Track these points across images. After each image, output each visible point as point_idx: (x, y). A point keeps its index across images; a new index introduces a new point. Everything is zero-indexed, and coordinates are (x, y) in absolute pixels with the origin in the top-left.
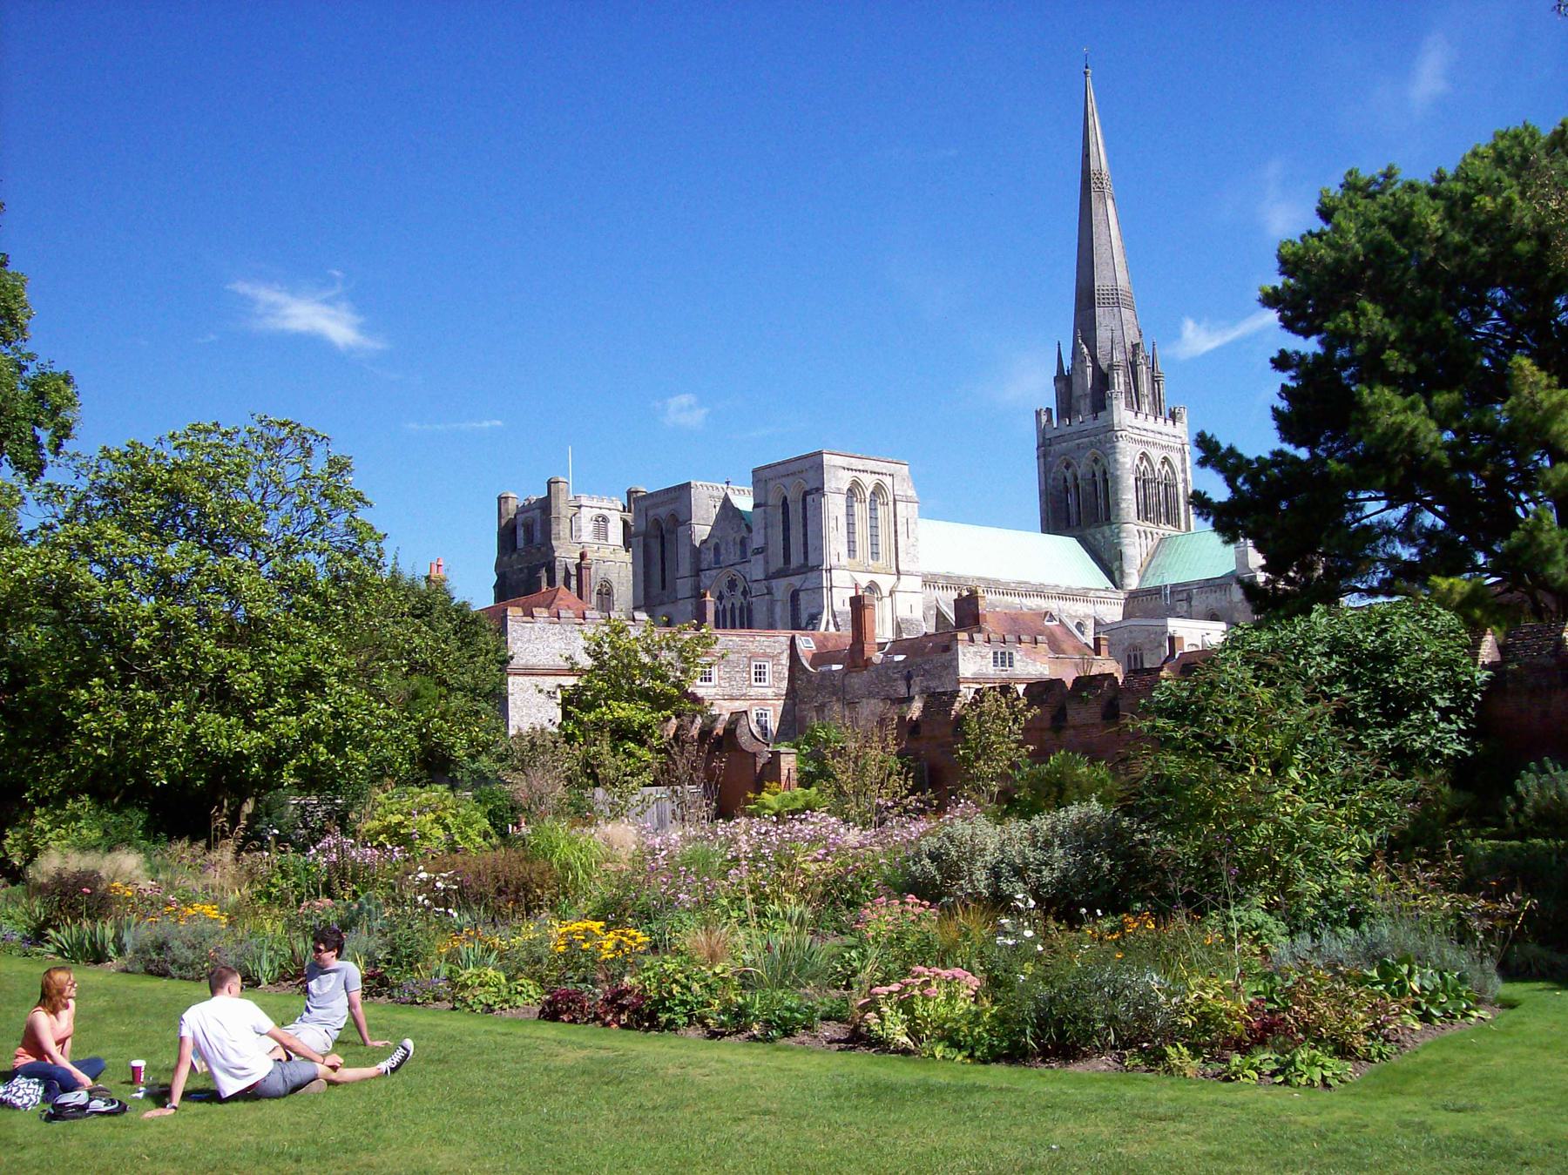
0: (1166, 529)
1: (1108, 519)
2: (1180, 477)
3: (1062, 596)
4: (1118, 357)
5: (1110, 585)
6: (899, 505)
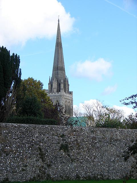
4: (62, 81)
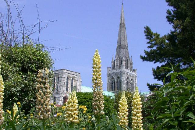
1: (120, 89)
2: (135, 83)
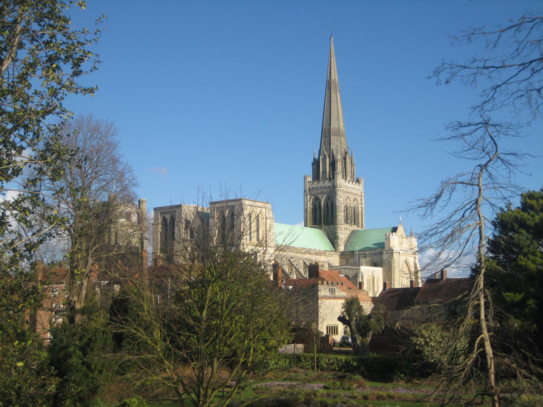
0: (354, 228)
3: (317, 254)
5: (333, 249)
6: (268, 220)
